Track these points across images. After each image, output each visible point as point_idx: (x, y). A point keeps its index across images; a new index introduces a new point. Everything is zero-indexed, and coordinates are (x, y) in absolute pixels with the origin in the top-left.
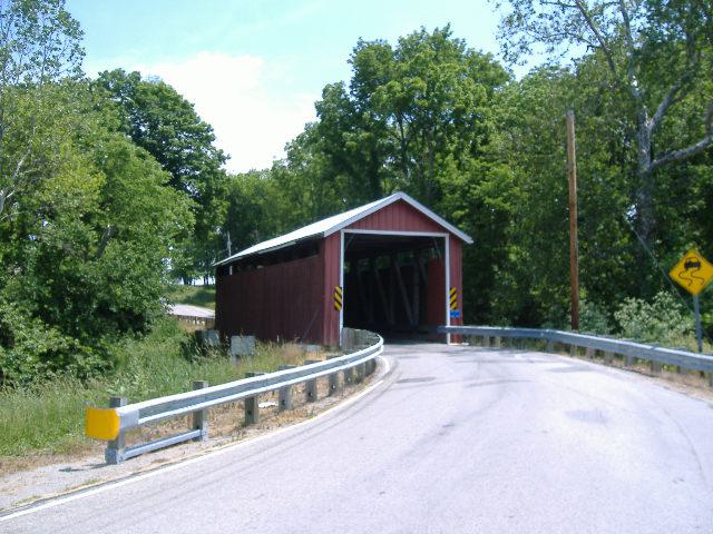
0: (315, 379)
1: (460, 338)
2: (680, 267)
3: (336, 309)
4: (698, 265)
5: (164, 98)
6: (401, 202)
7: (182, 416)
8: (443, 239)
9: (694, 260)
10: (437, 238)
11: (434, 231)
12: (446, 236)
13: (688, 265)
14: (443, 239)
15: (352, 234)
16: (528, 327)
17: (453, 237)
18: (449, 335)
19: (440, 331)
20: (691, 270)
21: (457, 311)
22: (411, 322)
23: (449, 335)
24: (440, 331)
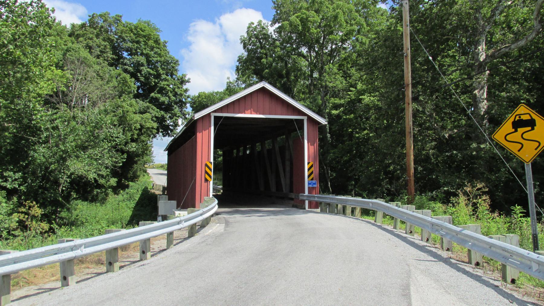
0: (149, 239)
1: (315, 205)
2: (507, 126)
3: (206, 180)
4: (531, 123)
5: (138, 35)
6: (263, 89)
7: (54, 262)
8: (302, 121)
9: (525, 117)
10: (296, 120)
11: (299, 115)
12: (305, 118)
13: (517, 125)
14: (302, 121)
15: (221, 117)
16: (344, 195)
17: (310, 119)
18: (307, 202)
19: (301, 198)
20: (521, 130)
21: (314, 181)
22: (284, 190)
23: (307, 202)
24: (301, 198)
